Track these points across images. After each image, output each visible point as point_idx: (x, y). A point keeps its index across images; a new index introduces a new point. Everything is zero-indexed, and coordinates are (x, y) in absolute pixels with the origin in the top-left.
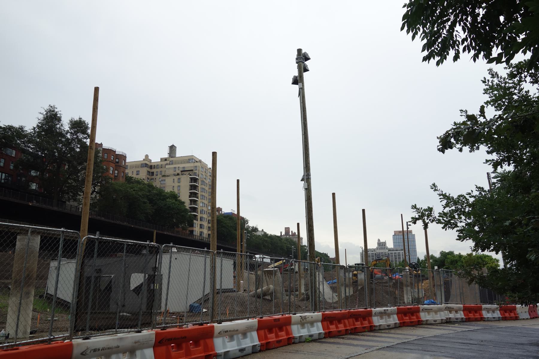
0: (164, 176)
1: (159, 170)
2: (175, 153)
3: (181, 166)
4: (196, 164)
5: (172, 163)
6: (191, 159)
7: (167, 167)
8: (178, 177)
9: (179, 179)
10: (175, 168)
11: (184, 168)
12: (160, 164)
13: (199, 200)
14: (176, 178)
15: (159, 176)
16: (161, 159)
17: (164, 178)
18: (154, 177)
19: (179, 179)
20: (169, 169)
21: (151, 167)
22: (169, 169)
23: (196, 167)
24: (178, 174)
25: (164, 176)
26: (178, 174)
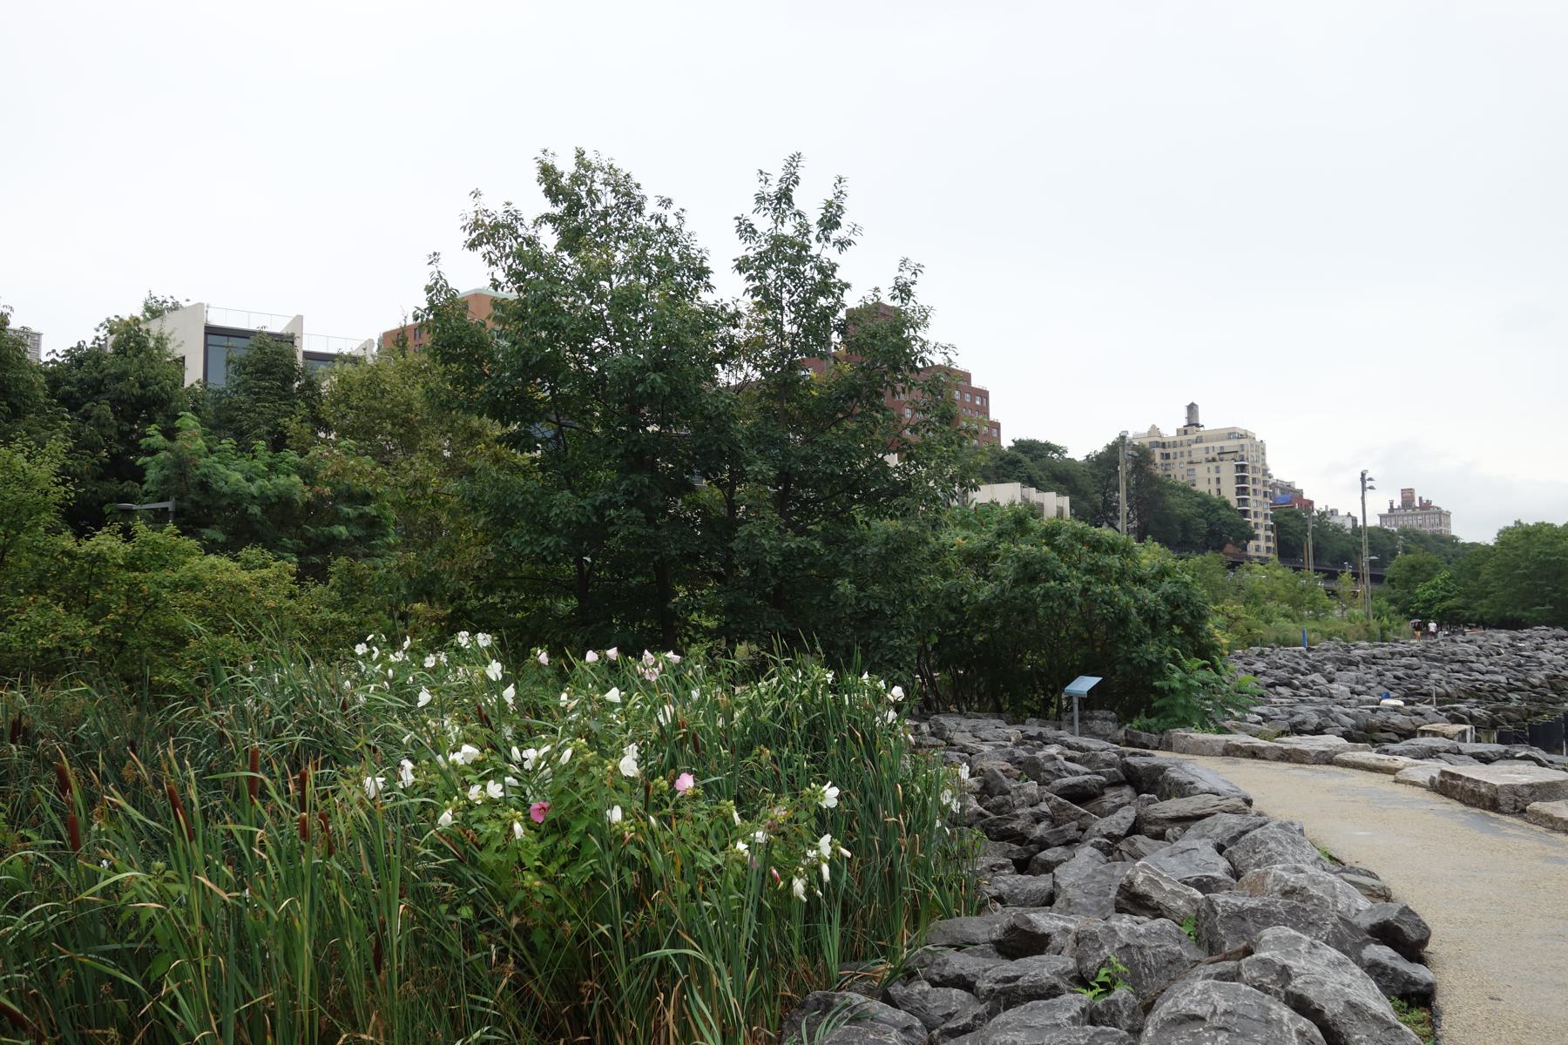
0: (1191, 463)
1: (1178, 450)
2: (1197, 417)
3: (1218, 445)
4: (1242, 441)
5: (1199, 440)
6: (1232, 434)
7: (1194, 446)
8: (1215, 464)
9: (1217, 468)
10: (1207, 448)
11: (1222, 448)
12: (1178, 439)
13: (1251, 497)
14: (1212, 466)
15: (1179, 459)
16: (1178, 431)
17: (1192, 466)
18: (1171, 460)
19: (1217, 468)
20: (1198, 452)
21: (1163, 445)
22: (1198, 452)
23: (1242, 446)
24: (1214, 460)
25: (1191, 463)
26: (1214, 460)
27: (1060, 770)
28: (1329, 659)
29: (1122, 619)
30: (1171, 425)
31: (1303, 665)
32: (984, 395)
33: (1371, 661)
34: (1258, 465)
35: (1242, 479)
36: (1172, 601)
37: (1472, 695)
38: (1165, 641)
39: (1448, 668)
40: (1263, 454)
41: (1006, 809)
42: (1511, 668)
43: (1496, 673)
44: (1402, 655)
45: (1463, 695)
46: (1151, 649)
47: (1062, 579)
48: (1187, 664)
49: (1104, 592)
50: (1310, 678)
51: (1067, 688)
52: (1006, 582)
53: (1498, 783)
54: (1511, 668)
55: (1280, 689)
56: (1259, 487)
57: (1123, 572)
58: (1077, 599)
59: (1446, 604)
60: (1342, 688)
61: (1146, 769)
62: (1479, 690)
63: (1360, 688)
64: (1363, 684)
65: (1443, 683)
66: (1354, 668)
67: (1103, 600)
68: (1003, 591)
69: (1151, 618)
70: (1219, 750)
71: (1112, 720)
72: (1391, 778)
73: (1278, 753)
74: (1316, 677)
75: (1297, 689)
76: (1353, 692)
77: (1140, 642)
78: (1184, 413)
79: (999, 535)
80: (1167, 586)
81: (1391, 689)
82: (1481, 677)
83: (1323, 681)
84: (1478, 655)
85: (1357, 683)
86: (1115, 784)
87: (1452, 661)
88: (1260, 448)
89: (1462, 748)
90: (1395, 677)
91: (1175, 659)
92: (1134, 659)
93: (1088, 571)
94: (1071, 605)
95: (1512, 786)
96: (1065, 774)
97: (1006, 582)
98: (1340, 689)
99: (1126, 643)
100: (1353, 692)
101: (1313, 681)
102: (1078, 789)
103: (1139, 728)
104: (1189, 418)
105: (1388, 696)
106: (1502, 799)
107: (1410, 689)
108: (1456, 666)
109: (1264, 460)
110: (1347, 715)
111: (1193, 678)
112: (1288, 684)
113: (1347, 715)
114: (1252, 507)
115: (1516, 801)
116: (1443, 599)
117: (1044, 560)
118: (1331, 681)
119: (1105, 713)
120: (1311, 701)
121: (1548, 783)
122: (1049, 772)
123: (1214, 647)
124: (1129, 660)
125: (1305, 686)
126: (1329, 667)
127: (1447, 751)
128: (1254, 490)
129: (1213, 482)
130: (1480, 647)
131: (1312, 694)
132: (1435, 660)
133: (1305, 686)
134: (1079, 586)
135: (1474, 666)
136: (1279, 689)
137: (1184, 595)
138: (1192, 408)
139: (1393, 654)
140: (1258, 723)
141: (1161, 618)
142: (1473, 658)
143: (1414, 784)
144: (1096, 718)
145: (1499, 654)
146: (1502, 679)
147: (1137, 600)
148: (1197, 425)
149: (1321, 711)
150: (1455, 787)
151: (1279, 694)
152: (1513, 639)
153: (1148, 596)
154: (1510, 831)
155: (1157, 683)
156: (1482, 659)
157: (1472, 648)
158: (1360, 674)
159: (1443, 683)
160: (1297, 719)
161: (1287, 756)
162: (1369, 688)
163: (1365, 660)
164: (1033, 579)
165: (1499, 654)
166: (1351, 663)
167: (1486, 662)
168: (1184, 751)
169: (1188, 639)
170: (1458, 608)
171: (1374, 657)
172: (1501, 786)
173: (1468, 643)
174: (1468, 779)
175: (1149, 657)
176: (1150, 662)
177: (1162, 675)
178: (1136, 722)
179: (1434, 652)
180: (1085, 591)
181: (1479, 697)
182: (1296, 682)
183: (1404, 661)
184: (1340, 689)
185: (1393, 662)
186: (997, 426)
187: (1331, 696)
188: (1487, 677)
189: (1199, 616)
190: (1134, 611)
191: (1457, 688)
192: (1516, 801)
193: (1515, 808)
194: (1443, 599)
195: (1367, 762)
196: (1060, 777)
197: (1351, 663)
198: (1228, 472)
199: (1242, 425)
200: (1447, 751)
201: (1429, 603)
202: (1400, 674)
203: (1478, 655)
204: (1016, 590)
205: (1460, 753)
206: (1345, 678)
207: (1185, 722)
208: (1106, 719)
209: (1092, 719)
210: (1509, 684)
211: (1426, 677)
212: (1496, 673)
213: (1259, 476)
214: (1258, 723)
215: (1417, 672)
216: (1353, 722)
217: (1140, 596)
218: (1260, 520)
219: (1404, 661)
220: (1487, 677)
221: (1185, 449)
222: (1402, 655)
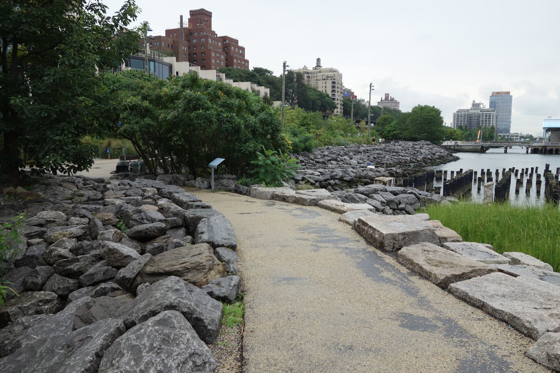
0: (317, 80)
1: (313, 75)
3: (326, 74)
4: (335, 73)
5: (320, 72)
6: (332, 70)
7: (318, 74)
11: (328, 75)
12: (313, 71)
13: (336, 94)
14: (324, 81)
16: (313, 68)
17: (317, 81)
18: (310, 79)
20: (320, 76)
21: (308, 73)
22: (320, 76)
24: (325, 79)
25: (317, 80)
26: (325, 79)
27: (142, 219)
28: (352, 151)
29: (237, 130)
30: (311, 66)
31: (342, 152)
32: (243, 49)
33: (366, 151)
34: (339, 82)
35: (334, 87)
36: (263, 122)
37: (398, 164)
38: (259, 142)
39: (391, 154)
40: (341, 78)
41: (81, 251)
42: (412, 154)
43: (407, 156)
44: (377, 149)
45: (395, 164)
46: (251, 145)
47: (208, 109)
48: (267, 152)
49: (227, 117)
50: (344, 157)
51: (210, 164)
52: (179, 110)
53: (385, 232)
54: (412, 154)
55: (332, 162)
56: (339, 90)
57: (240, 108)
58: (214, 119)
59: (394, 132)
60: (354, 161)
61: (192, 218)
62: (401, 162)
63: (361, 161)
64: (362, 160)
65: (389, 160)
66: (360, 154)
67: (227, 121)
68: (179, 115)
69: (254, 132)
70: (269, 196)
71: (233, 179)
72: (339, 216)
73: (294, 199)
74: (346, 157)
75: (339, 162)
76: (358, 163)
77: (246, 142)
78: (316, 62)
79: (183, 87)
80: (262, 115)
81: (372, 162)
82: (402, 158)
83: (348, 159)
84: (402, 150)
85: (360, 160)
86: (175, 227)
87: (393, 152)
88: (340, 76)
89: (387, 189)
90: (374, 158)
91: (262, 152)
92: (242, 150)
93: (222, 106)
94: (211, 122)
95: (393, 235)
96: (145, 221)
97: (179, 110)
98: (354, 162)
99: (239, 142)
100: (358, 163)
101: (345, 159)
102: (142, 234)
103: (241, 184)
104: (317, 64)
105: (369, 164)
106: (386, 242)
107: (378, 162)
108: (394, 154)
109: (341, 80)
110: (353, 172)
111: (269, 159)
112: (336, 160)
113: (353, 172)
114: (336, 97)
115: (394, 243)
116: (394, 130)
117: (198, 99)
118: (351, 159)
119: (229, 176)
120: (41, 225)
121: (413, 232)
122: (135, 220)
123: (284, 145)
124: (240, 150)
125: (342, 161)
126: (351, 154)
127: (381, 191)
128: (338, 91)
129: (324, 87)
130: (403, 147)
131: (344, 164)
132: (388, 151)
133: (342, 161)
134: (215, 113)
135: (400, 154)
136: (332, 162)
137: (270, 120)
138: (318, 60)
139: (374, 149)
140: (319, 176)
141: (258, 131)
142: (400, 151)
143: (347, 223)
144: (224, 178)
145: (409, 150)
146: (409, 158)
147: (246, 121)
148: (320, 66)
149: (343, 171)
150: (364, 230)
151: (332, 164)
152: (414, 145)
153: (252, 119)
154: (386, 274)
155: (252, 162)
156: (403, 151)
157: (400, 148)
158: (362, 156)
159: (389, 160)
160: (334, 174)
161: (298, 201)
162: (364, 161)
163: (364, 151)
164: (195, 108)
165: (409, 150)
166: (359, 152)
167: (404, 153)
168: (255, 197)
169: (271, 141)
170: (398, 134)
171: (367, 150)
172: (387, 235)
173: (398, 146)
174: (370, 227)
175: (250, 149)
176: (250, 152)
177: (256, 157)
178: (240, 181)
179: (388, 149)
180: (218, 115)
181: (401, 165)
182: (338, 159)
183: (377, 152)
184: (354, 162)
185: (373, 152)
186: (248, 62)
187: (350, 165)
188: (404, 158)
189: (276, 130)
190: (243, 126)
191: (394, 162)
192: (394, 243)
193: (393, 248)
194: (394, 130)
195: (331, 206)
196: (142, 224)
197: (359, 152)
198: (329, 84)
199: (335, 67)
200: (381, 191)
201: (389, 132)
202: (375, 156)
203: (402, 150)
204: (184, 114)
205: (386, 191)
206: (356, 158)
207: (259, 182)
208: (229, 179)
209: (222, 178)
210: (411, 160)
211: (384, 158)
212: (407, 156)
213: (339, 86)
214: (319, 176)
215: (381, 156)
216: (355, 175)
217: (247, 119)
218: (339, 102)
219: (377, 152)
220: (404, 158)
221: (315, 75)
222: (377, 149)
